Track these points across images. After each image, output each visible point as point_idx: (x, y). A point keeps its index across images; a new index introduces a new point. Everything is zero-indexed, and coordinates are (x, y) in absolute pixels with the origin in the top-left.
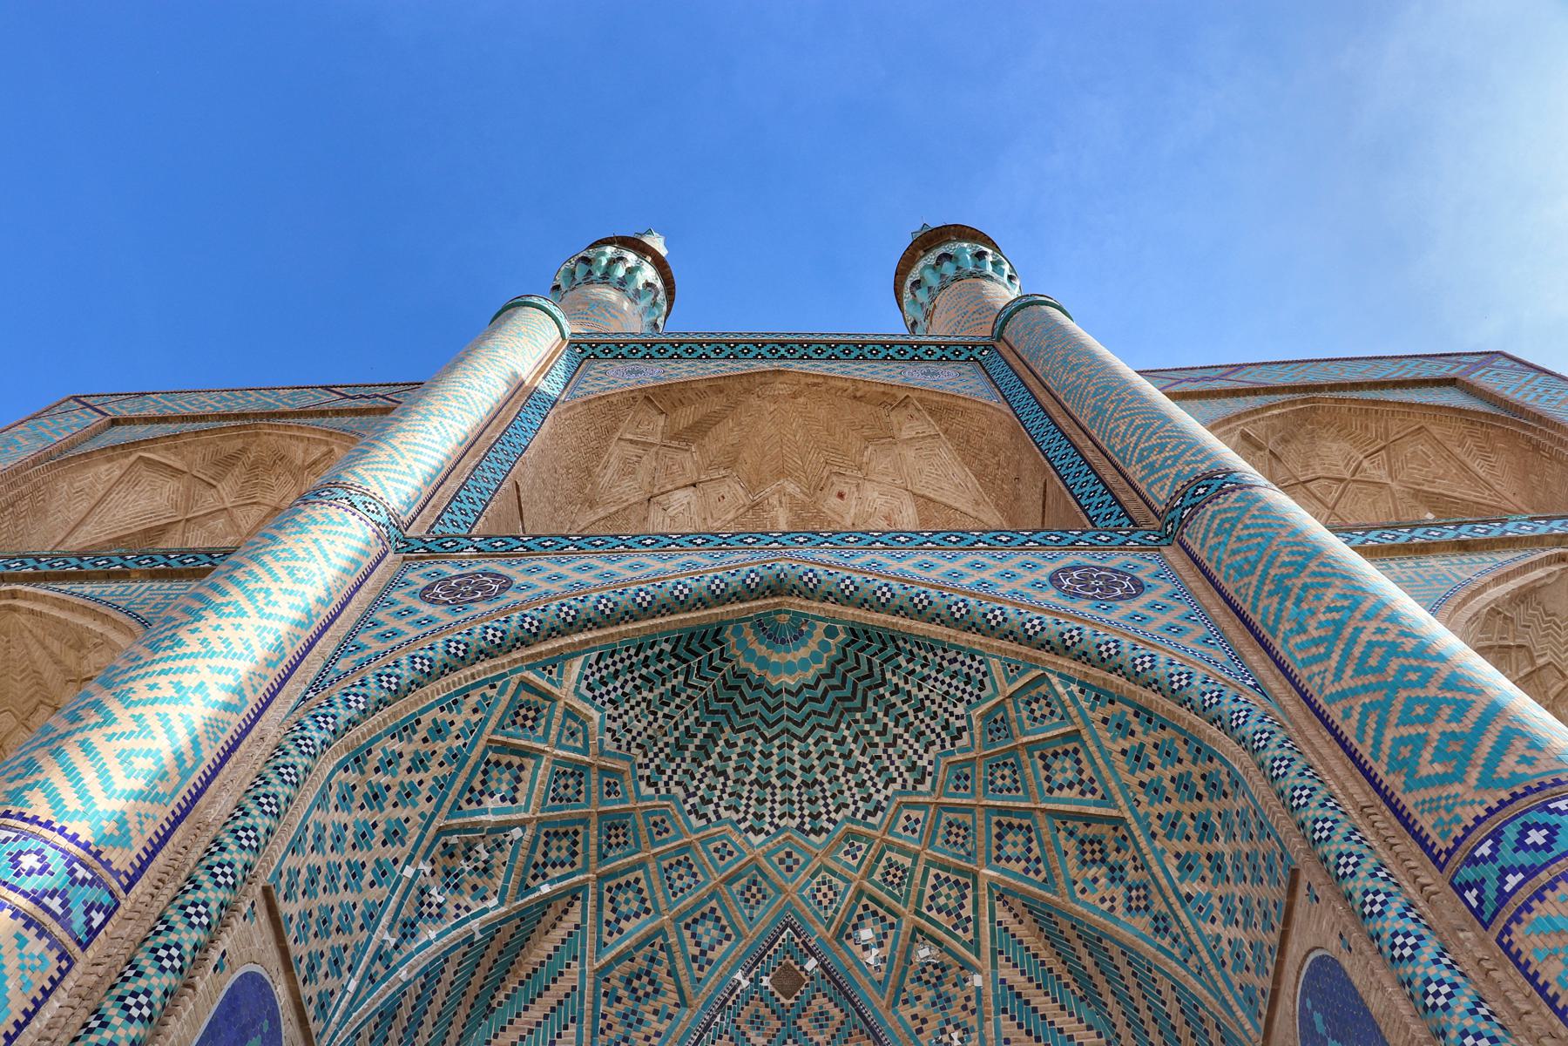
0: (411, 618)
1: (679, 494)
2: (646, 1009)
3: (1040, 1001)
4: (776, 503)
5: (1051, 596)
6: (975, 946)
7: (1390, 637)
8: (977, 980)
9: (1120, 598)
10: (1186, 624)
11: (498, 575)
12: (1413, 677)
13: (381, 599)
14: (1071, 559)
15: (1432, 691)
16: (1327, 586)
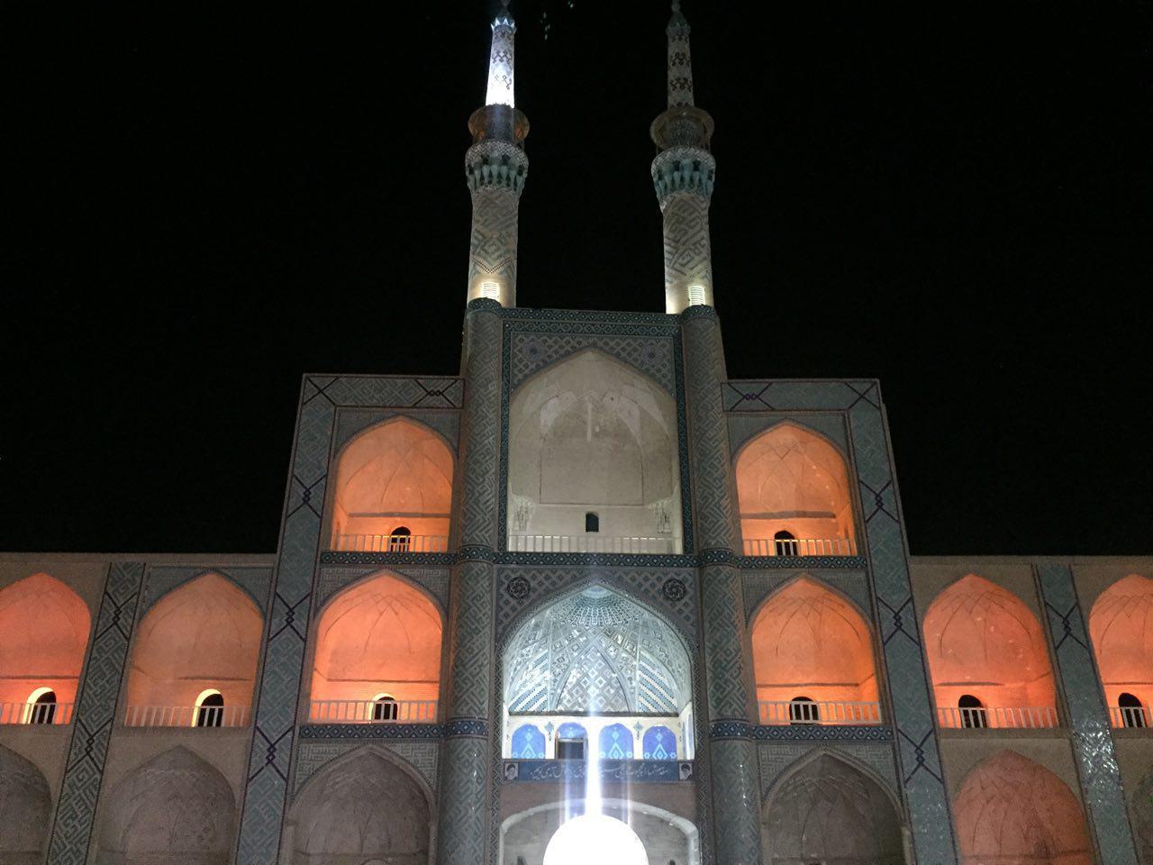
0: (509, 606)
1: (552, 401)
2: (562, 664)
3: (648, 667)
4: (587, 399)
5: (661, 598)
6: (635, 657)
7: (722, 660)
8: (635, 663)
9: (678, 600)
10: (691, 615)
11: (525, 580)
12: (721, 676)
13: (500, 596)
14: (672, 572)
15: (721, 682)
16: (718, 630)
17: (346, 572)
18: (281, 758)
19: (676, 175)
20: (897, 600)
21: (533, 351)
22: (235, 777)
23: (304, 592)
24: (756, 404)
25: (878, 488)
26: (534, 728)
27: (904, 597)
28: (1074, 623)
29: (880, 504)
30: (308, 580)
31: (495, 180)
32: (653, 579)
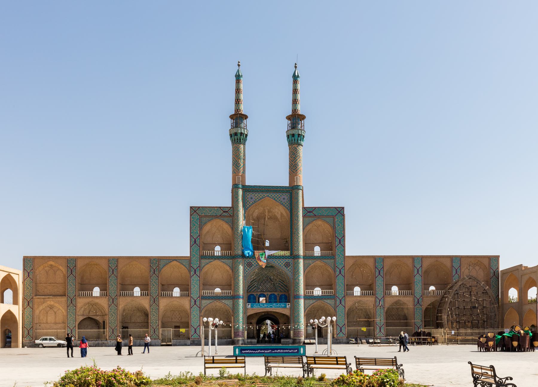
17: (207, 261)
18: (198, 303)
19: (293, 138)
20: (340, 267)
21: (252, 198)
22: (187, 306)
23: (198, 266)
24: (311, 214)
25: (340, 238)
26: (253, 295)
27: (343, 266)
28: (381, 272)
29: (340, 242)
30: (198, 263)
31: (239, 141)
32: (282, 262)
